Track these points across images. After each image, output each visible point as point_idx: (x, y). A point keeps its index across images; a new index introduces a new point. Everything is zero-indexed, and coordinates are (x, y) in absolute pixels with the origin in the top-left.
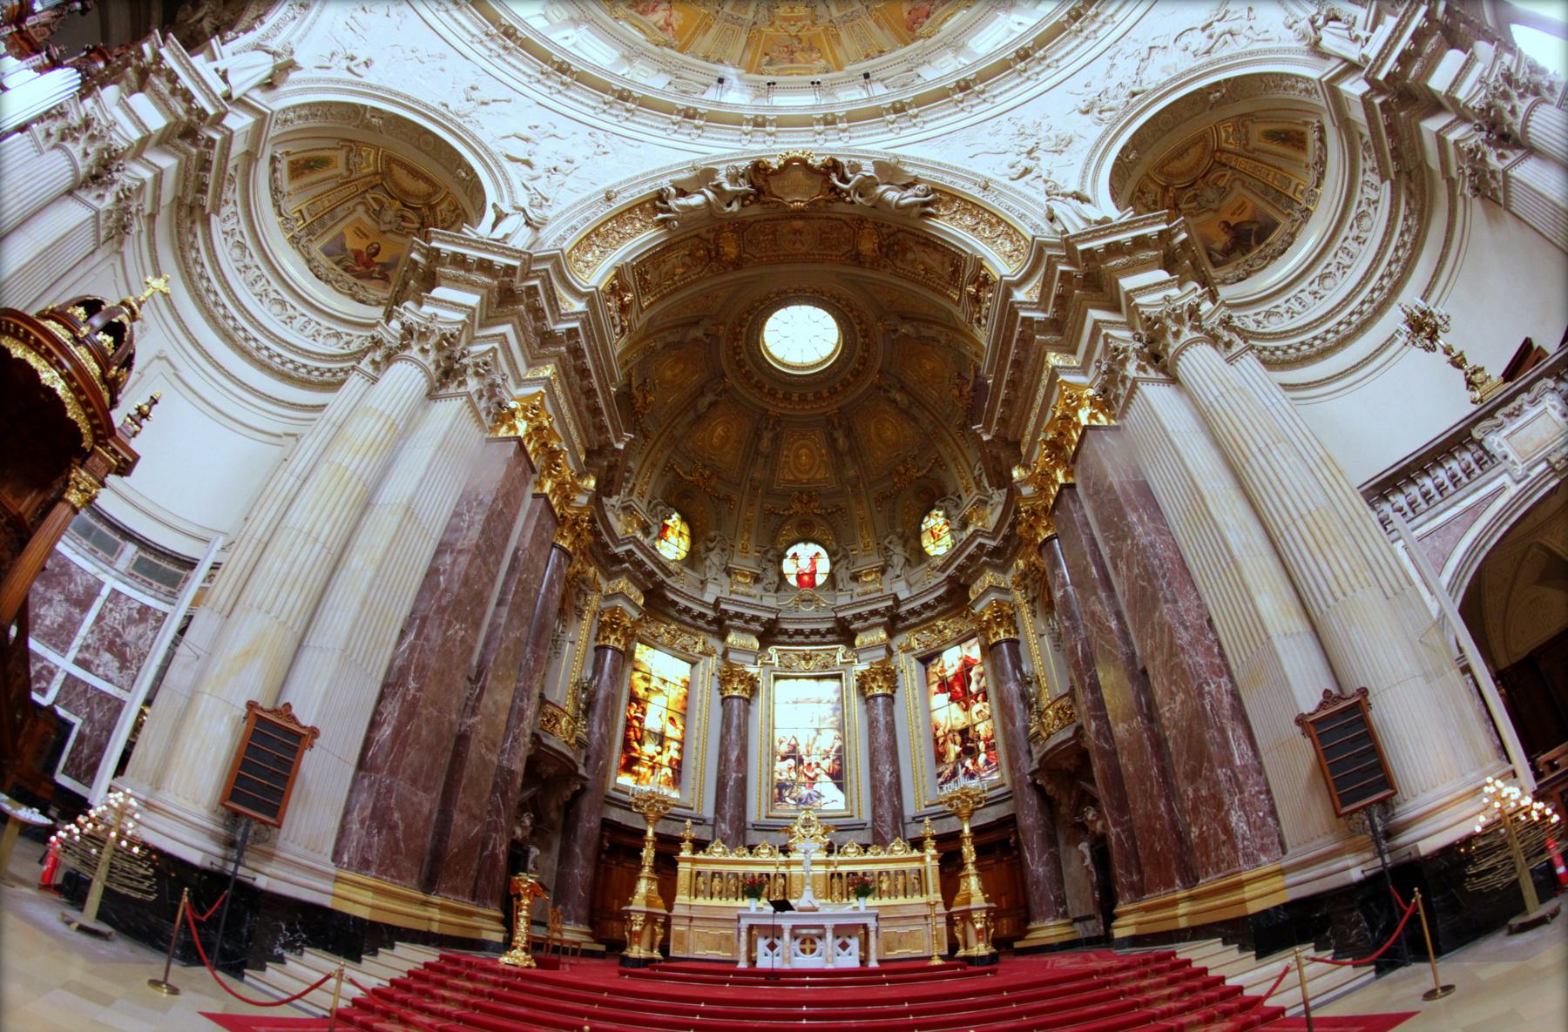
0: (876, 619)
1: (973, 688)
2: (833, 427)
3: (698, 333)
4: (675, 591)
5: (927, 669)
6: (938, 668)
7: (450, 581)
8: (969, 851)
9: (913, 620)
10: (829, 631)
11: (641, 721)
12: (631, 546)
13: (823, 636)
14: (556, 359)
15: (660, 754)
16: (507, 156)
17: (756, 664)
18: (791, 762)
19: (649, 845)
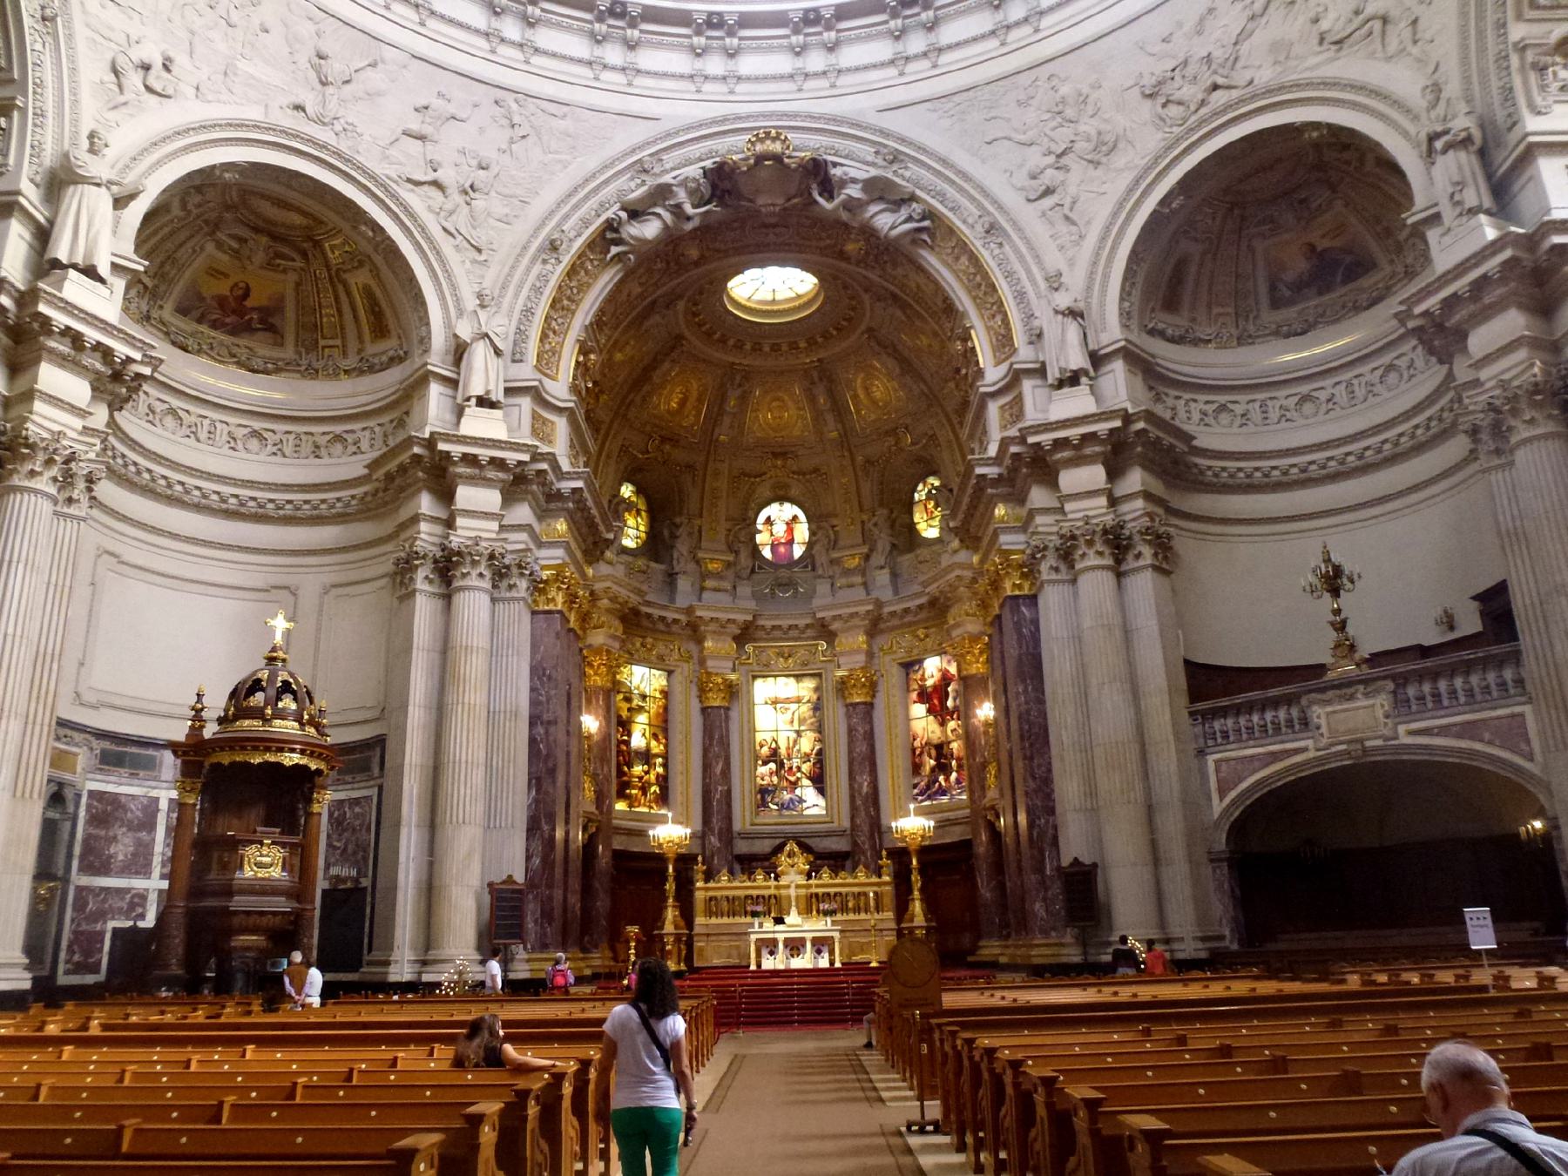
0: (856, 621)
1: (950, 703)
2: (813, 383)
3: (656, 318)
4: (648, 604)
5: (908, 674)
6: (918, 676)
7: (548, 746)
8: (916, 879)
9: (896, 622)
10: (807, 626)
11: (627, 743)
12: (608, 584)
13: (803, 632)
14: (565, 513)
15: (647, 773)
16: (409, 180)
17: (734, 670)
18: (772, 766)
19: (671, 879)
